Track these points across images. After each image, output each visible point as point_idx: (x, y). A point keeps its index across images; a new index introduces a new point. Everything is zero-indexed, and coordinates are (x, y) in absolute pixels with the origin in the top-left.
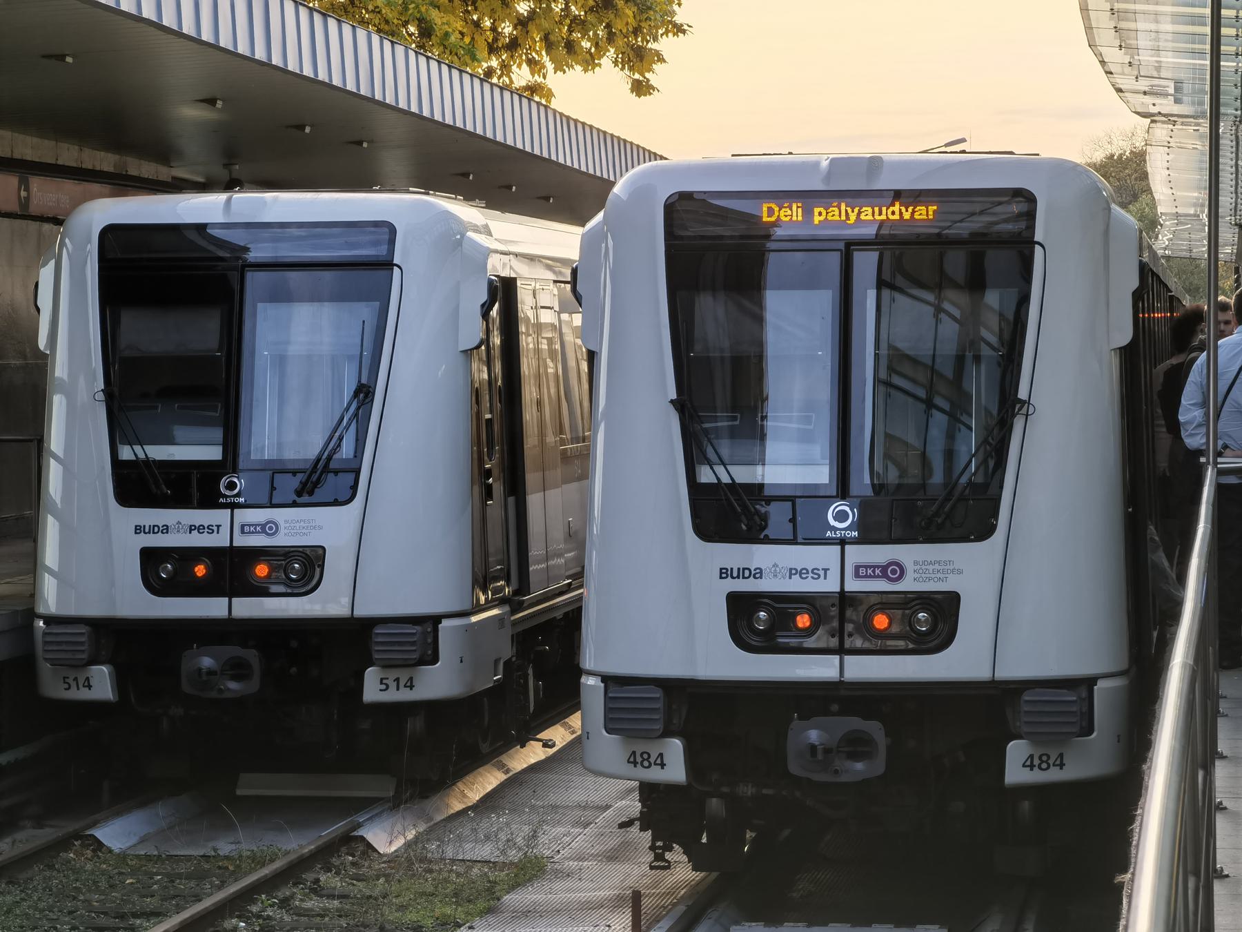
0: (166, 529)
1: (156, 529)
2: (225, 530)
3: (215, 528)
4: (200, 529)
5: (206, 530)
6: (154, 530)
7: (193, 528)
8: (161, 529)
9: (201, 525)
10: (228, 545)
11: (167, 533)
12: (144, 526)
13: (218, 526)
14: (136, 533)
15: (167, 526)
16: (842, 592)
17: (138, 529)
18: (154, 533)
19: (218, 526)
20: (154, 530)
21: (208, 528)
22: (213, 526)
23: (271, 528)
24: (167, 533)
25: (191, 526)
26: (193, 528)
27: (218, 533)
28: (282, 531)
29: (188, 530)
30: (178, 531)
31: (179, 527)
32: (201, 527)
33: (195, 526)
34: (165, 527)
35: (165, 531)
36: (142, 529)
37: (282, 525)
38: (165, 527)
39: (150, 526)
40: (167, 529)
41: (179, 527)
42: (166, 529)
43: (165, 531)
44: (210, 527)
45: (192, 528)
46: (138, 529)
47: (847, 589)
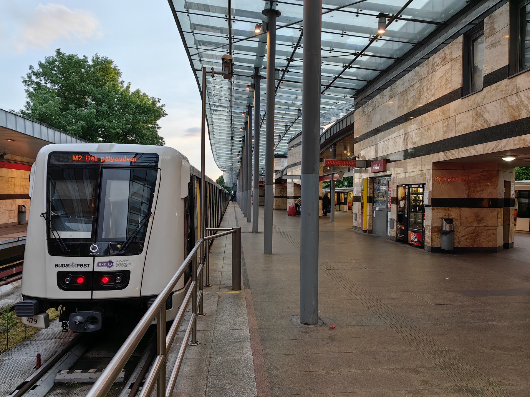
0: (68, 266)
1: (64, 266)
3: (87, 265)
4: (81, 265)
5: (84, 266)
6: (62, 266)
7: (78, 265)
8: (66, 265)
9: (82, 264)
10: (92, 271)
11: (68, 267)
12: (59, 264)
14: (56, 267)
15: (68, 264)
17: (57, 266)
18: (63, 267)
20: (62, 266)
21: (84, 265)
22: (86, 264)
24: (68, 267)
25: (77, 264)
26: (78, 265)
27: (88, 267)
28: (115, 265)
29: (76, 266)
31: (73, 265)
32: (82, 265)
33: (79, 264)
34: (67, 265)
35: (67, 266)
36: (58, 265)
37: (115, 263)
38: (67, 265)
39: (61, 264)
40: (68, 265)
41: (73, 265)
42: (68, 266)
43: (67, 266)
44: (85, 265)
46: (57, 266)
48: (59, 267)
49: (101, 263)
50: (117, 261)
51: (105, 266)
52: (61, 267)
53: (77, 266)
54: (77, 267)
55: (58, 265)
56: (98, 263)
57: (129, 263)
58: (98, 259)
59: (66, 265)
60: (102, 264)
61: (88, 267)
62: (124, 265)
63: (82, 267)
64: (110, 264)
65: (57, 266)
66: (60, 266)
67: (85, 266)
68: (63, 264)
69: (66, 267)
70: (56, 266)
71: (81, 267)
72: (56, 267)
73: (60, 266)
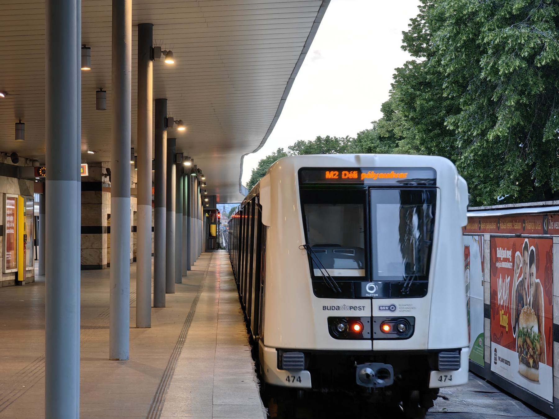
0: (338, 308)
1: (333, 308)
3: (362, 308)
4: (354, 308)
6: (332, 308)
8: (336, 308)
11: (339, 310)
12: (328, 307)
15: (339, 307)
16: (372, 317)
17: (325, 308)
18: (332, 309)
20: (332, 308)
23: (393, 308)
25: (350, 307)
27: (364, 310)
28: (398, 309)
29: (349, 309)
30: (345, 309)
36: (327, 308)
37: (398, 306)
39: (330, 307)
40: (339, 308)
42: (338, 308)
44: (360, 307)
46: (325, 308)
47: (374, 315)
48: (328, 309)
49: (383, 307)
50: (400, 305)
51: (387, 310)
52: (330, 309)
53: (350, 308)
54: (350, 310)
55: (327, 308)
57: (413, 308)
59: (337, 307)
61: (364, 310)
62: (408, 309)
63: (357, 310)
64: (393, 308)
65: (326, 308)
66: (329, 308)
67: (360, 309)
68: (332, 307)
69: (337, 309)
70: (323, 308)
71: (355, 310)
72: (323, 309)
73: (329, 308)
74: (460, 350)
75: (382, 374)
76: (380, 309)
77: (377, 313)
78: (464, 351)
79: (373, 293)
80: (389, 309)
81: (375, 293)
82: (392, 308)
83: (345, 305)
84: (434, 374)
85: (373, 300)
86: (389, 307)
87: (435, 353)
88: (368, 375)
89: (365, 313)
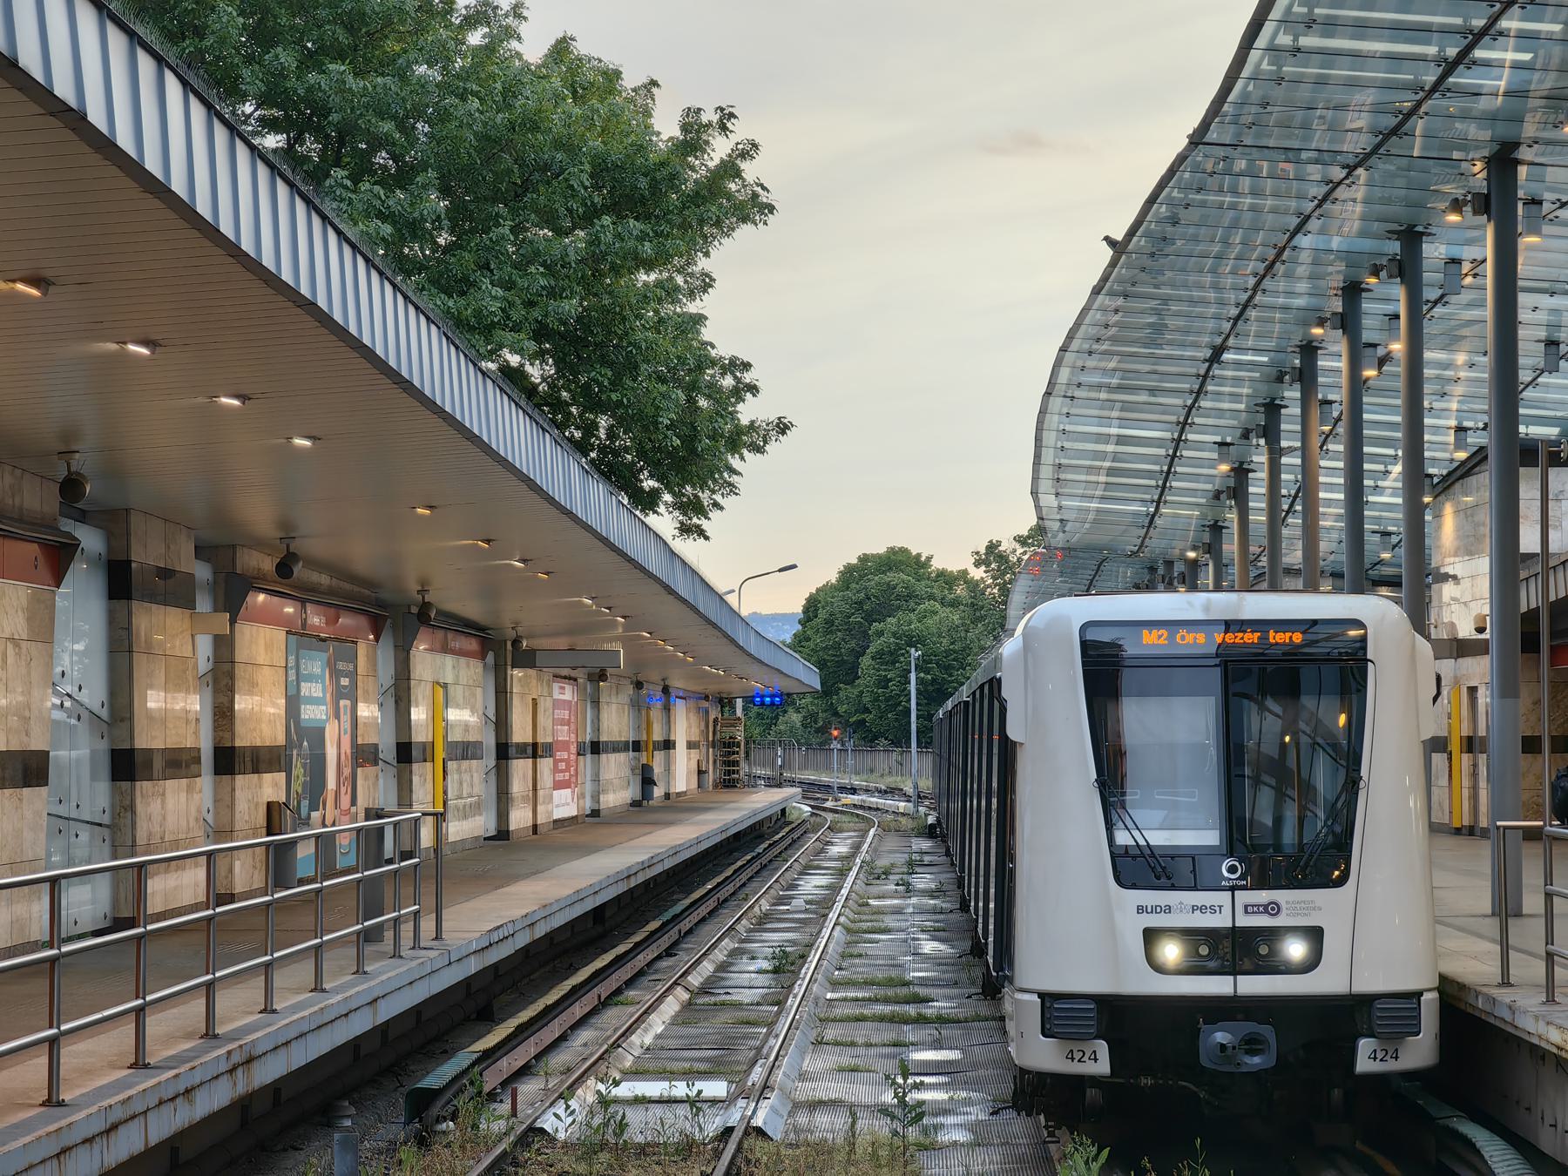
0: (1168, 910)
2: (1227, 910)
3: (1217, 909)
4: (1202, 909)
6: (1155, 910)
13: (1220, 907)
17: (1141, 909)
19: (1220, 907)
20: (1155, 910)
23: (1273, 909)
28: (1284, 911)
37: (1284, 906)
42: (1168, 910)
45: (1194, 909)
46: (1141, 909)
49: (1253, 906)
50: (1287, 902)
53: (1193, 910)
56: (1246, 907)
57: (1314, 909)
58: (1243, 897)
60: (1255, 909)
64: (1273, 909)
66: (1149, 910)
73: (1149, 910)
74: (1419, 994)
75: (1252, 1044)
76: (1246, 912)
77: (1243, 921)
78: (1427, 997)
79: (1236, 879)
80: (1266, 911)
81: (1241, 878)
82: (1272, 909)
83: (1181, 903)
84: (1365, 1046)
85: (1236, 892)
86: (1266, 907)
87: (1366, 1001)
88: (1223, 1047)
89: (1221, 921)
